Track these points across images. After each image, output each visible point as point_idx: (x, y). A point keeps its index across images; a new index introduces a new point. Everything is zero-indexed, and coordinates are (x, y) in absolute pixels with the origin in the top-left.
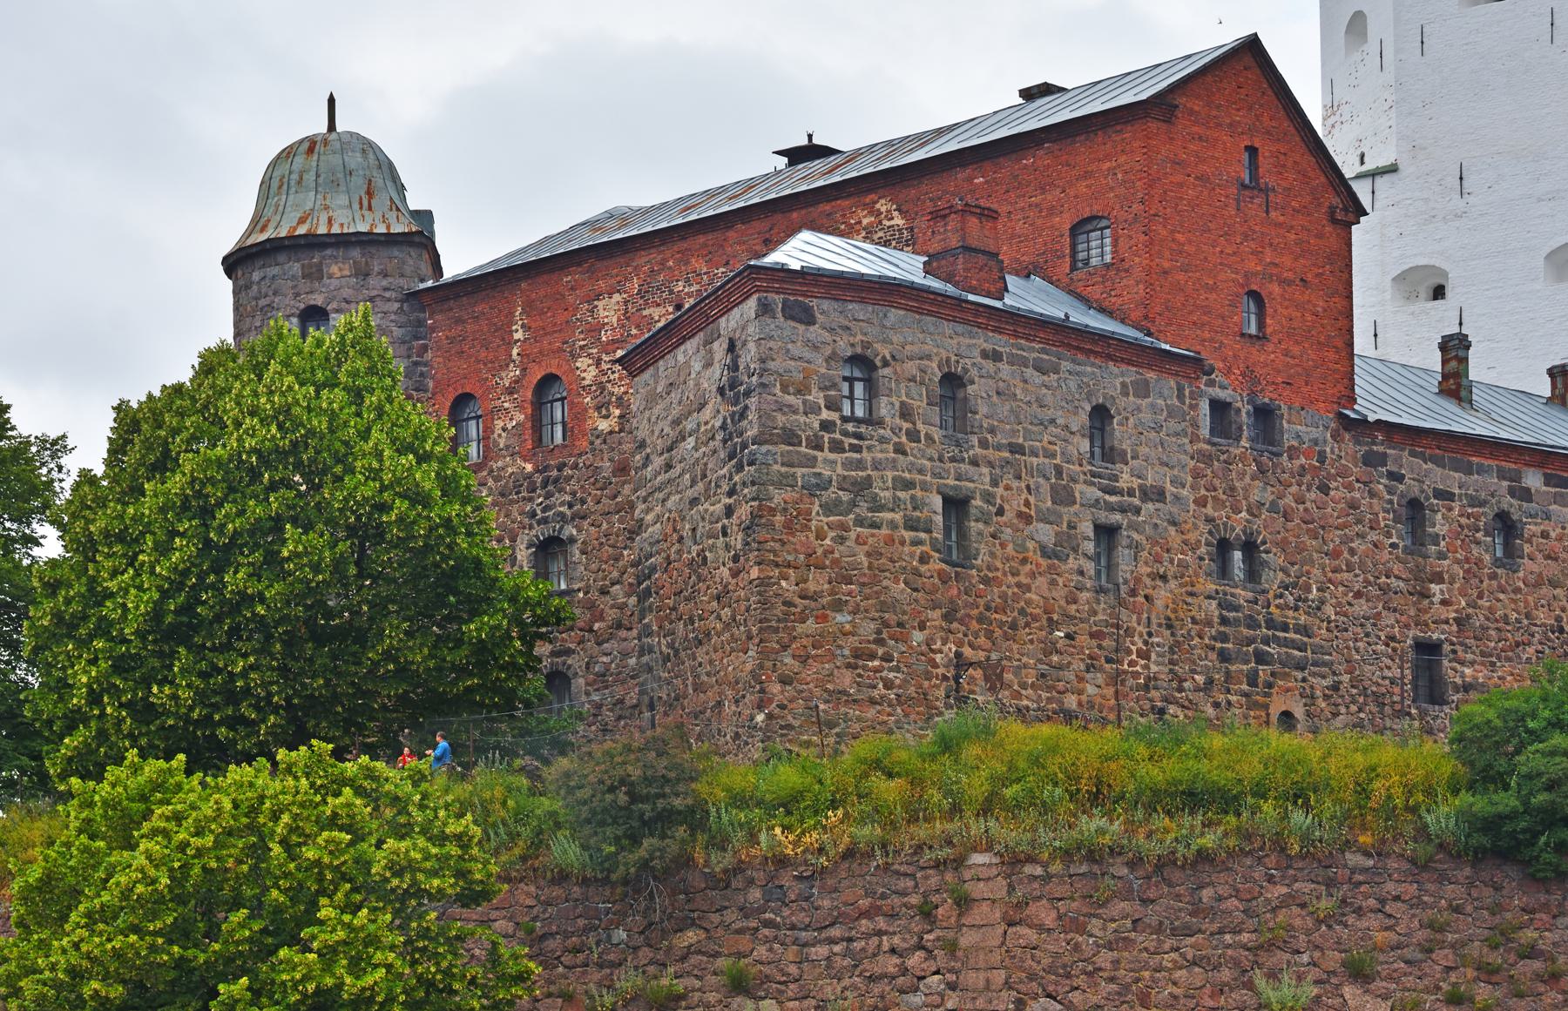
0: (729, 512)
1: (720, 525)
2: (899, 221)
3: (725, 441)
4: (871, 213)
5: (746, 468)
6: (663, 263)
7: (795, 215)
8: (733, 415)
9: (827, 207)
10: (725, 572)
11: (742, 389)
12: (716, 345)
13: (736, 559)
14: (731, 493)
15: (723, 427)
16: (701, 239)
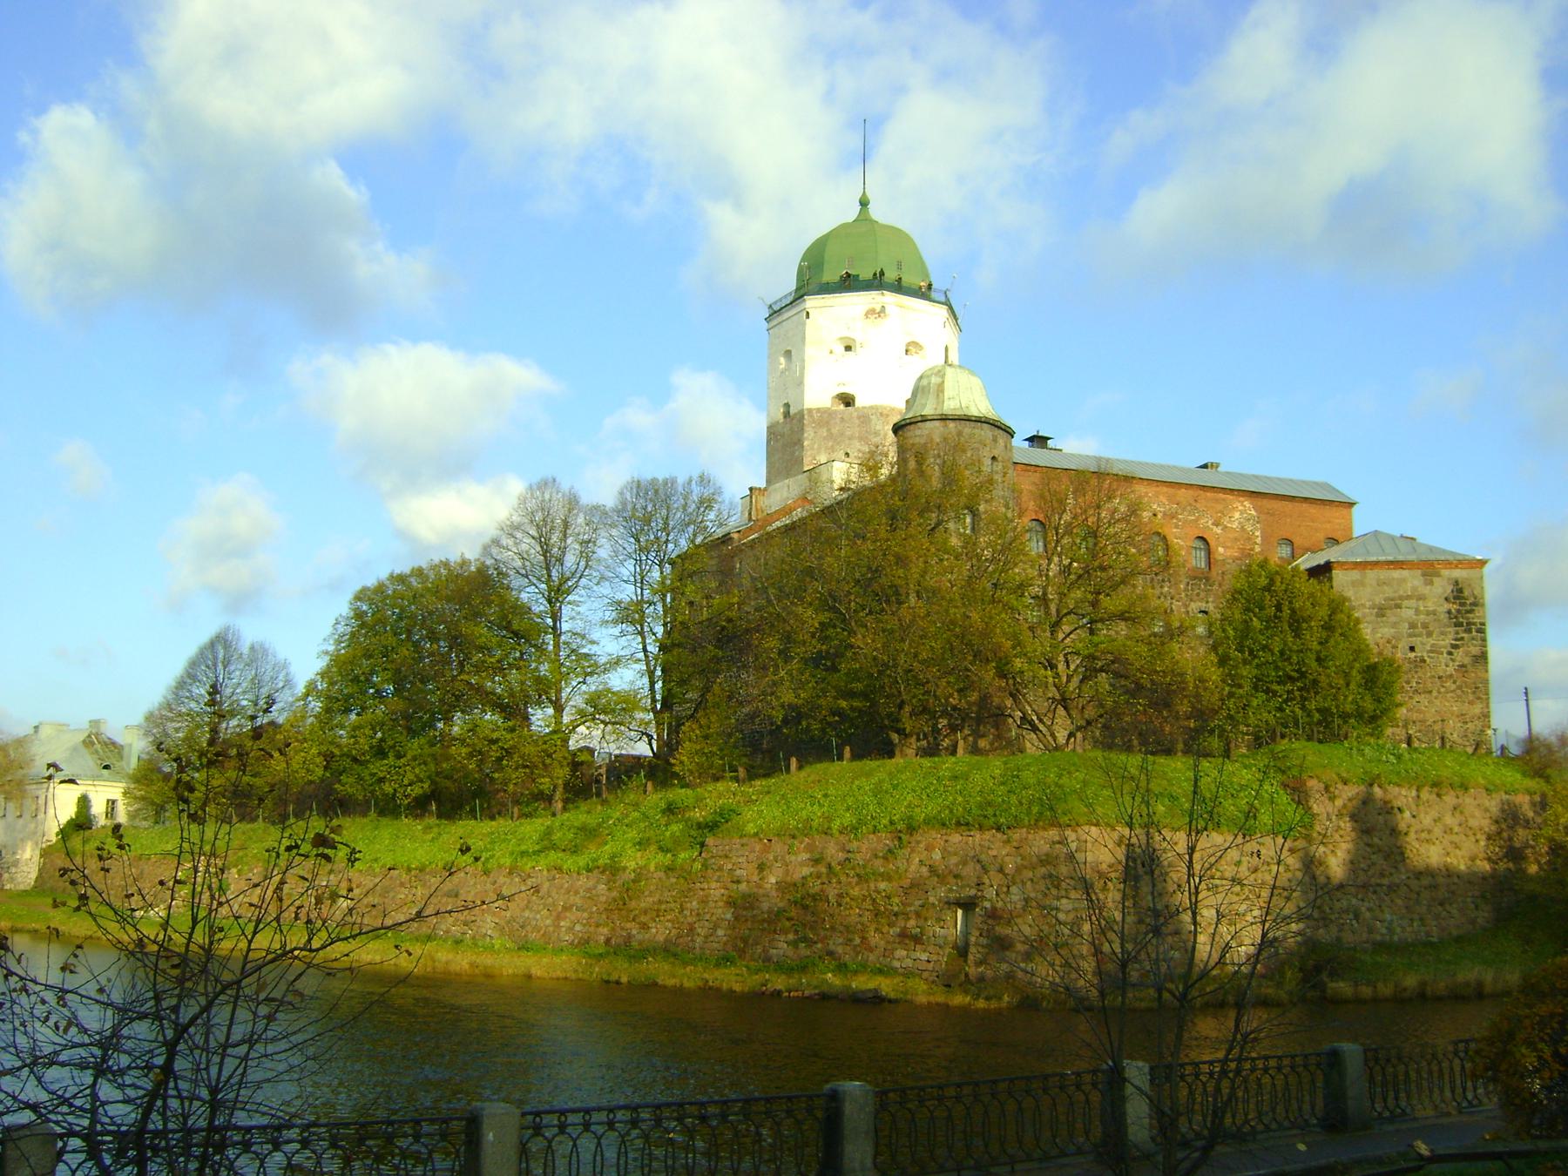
0: (1455, 647)
1: (1445, 651)
2: (1253, 512)
3: (1451, 618)
4: (1242, 505)
5: (1474, 633)
6: (1147, 493)
7: (1208, 494)
8: (1458, 611)
9: (1224, 496)
10: (1450, 670)
11: (1468, 602)
12: (1435, 580)
13: (1462, 666)
14: (1456, 640)
15: (1449, 612)
16: (1165, 489)
